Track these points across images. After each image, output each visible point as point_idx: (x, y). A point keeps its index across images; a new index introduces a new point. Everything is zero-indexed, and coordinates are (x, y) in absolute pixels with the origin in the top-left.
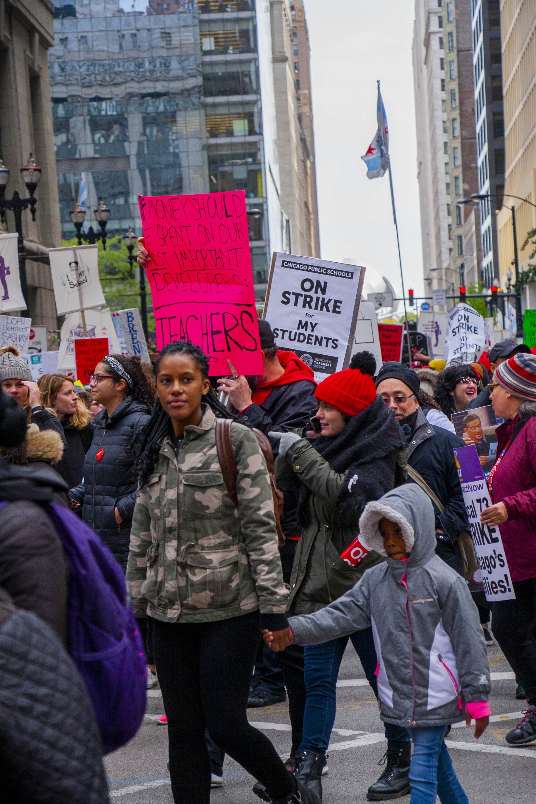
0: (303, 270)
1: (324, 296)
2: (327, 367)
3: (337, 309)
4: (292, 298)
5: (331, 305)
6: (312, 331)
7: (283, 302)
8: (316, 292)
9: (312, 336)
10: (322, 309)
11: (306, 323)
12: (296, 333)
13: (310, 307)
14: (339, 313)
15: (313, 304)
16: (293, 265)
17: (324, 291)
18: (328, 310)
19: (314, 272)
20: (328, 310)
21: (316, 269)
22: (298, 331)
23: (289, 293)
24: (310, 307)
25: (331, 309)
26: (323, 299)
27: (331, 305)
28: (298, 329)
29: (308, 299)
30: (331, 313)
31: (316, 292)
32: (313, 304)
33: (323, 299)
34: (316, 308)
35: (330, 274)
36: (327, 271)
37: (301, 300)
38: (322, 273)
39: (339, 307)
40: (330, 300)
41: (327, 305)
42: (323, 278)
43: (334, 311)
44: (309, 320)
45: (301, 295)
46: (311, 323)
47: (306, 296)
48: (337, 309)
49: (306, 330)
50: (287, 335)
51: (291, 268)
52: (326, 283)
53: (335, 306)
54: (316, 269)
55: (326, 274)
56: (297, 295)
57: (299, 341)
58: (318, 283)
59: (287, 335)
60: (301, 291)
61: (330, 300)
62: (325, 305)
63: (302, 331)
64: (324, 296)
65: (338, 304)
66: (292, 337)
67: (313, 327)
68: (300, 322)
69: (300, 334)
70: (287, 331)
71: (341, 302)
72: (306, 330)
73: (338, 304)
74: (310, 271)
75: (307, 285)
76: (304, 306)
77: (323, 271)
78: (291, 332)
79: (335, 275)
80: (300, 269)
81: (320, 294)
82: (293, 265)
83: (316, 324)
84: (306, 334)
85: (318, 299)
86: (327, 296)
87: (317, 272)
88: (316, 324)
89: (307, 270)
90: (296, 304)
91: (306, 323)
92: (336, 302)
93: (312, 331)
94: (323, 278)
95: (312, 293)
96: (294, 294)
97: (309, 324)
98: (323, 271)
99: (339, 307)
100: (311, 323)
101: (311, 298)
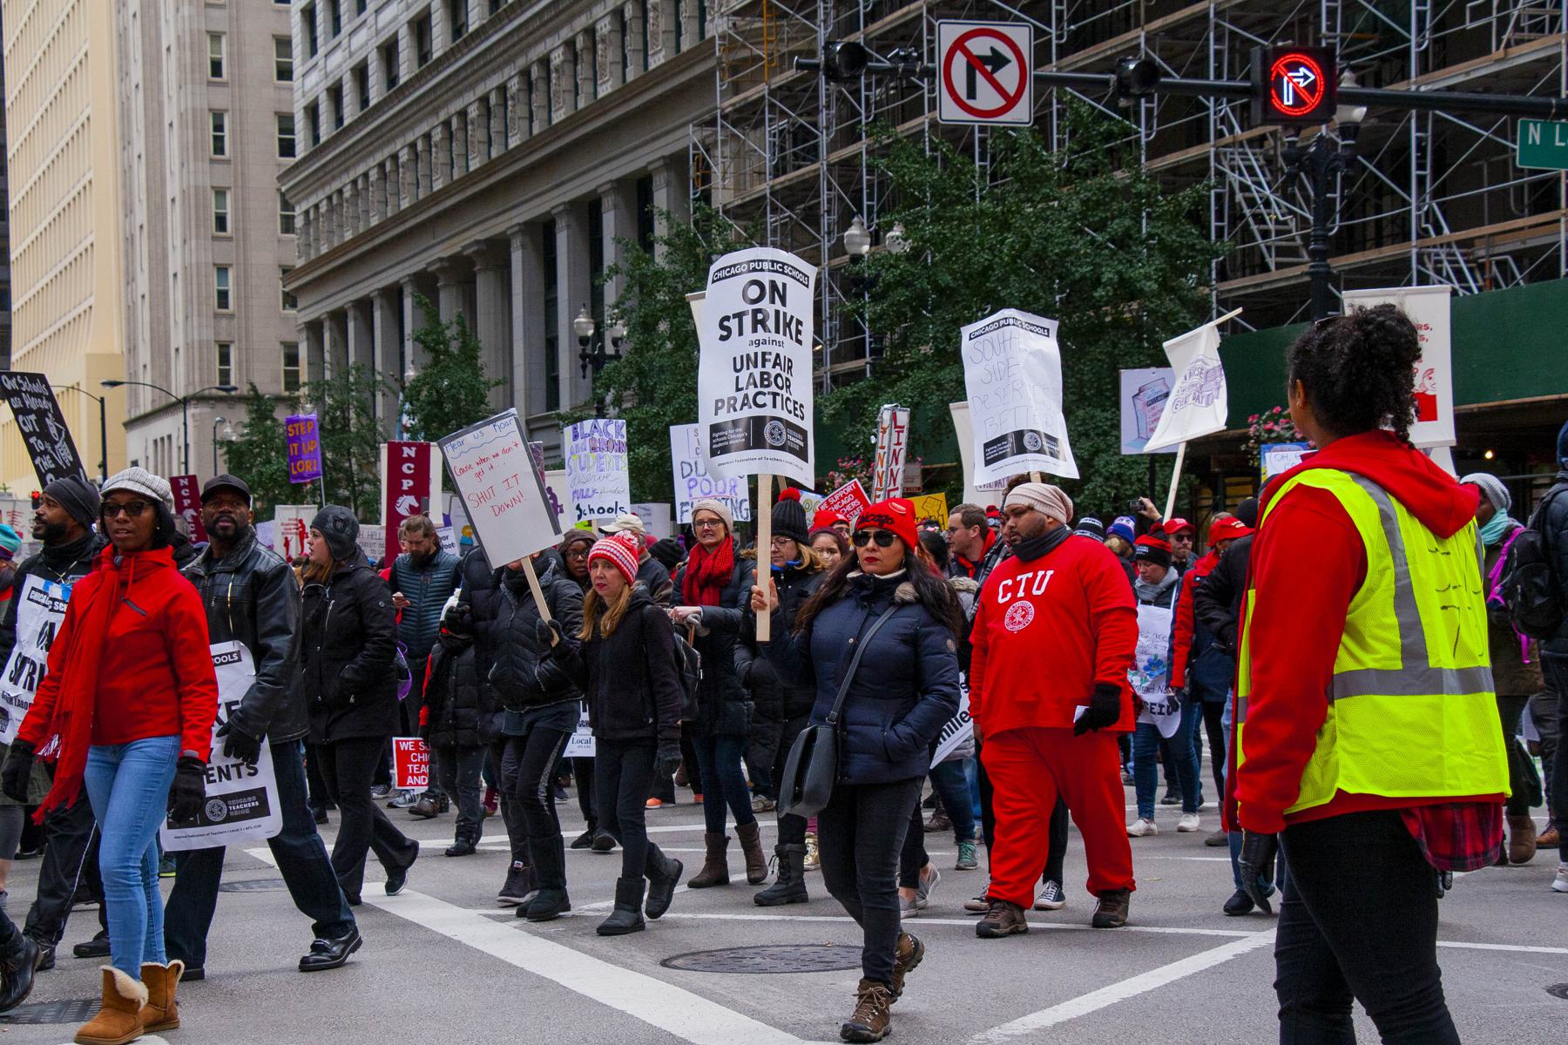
8: (773, 302)
13: (765, 329)
15: (771, 324)
26: (785, 314)
31: (773, 302)
32: (771, 324)
34: (777, 331)
37: (747, 320)
38: (777, 271)
52: (784, 285)
56: (739, 316)
76: (755, 330)
77: (777, 267)
85: (777, 312)
95: (765, 304)
96: (735, 316)
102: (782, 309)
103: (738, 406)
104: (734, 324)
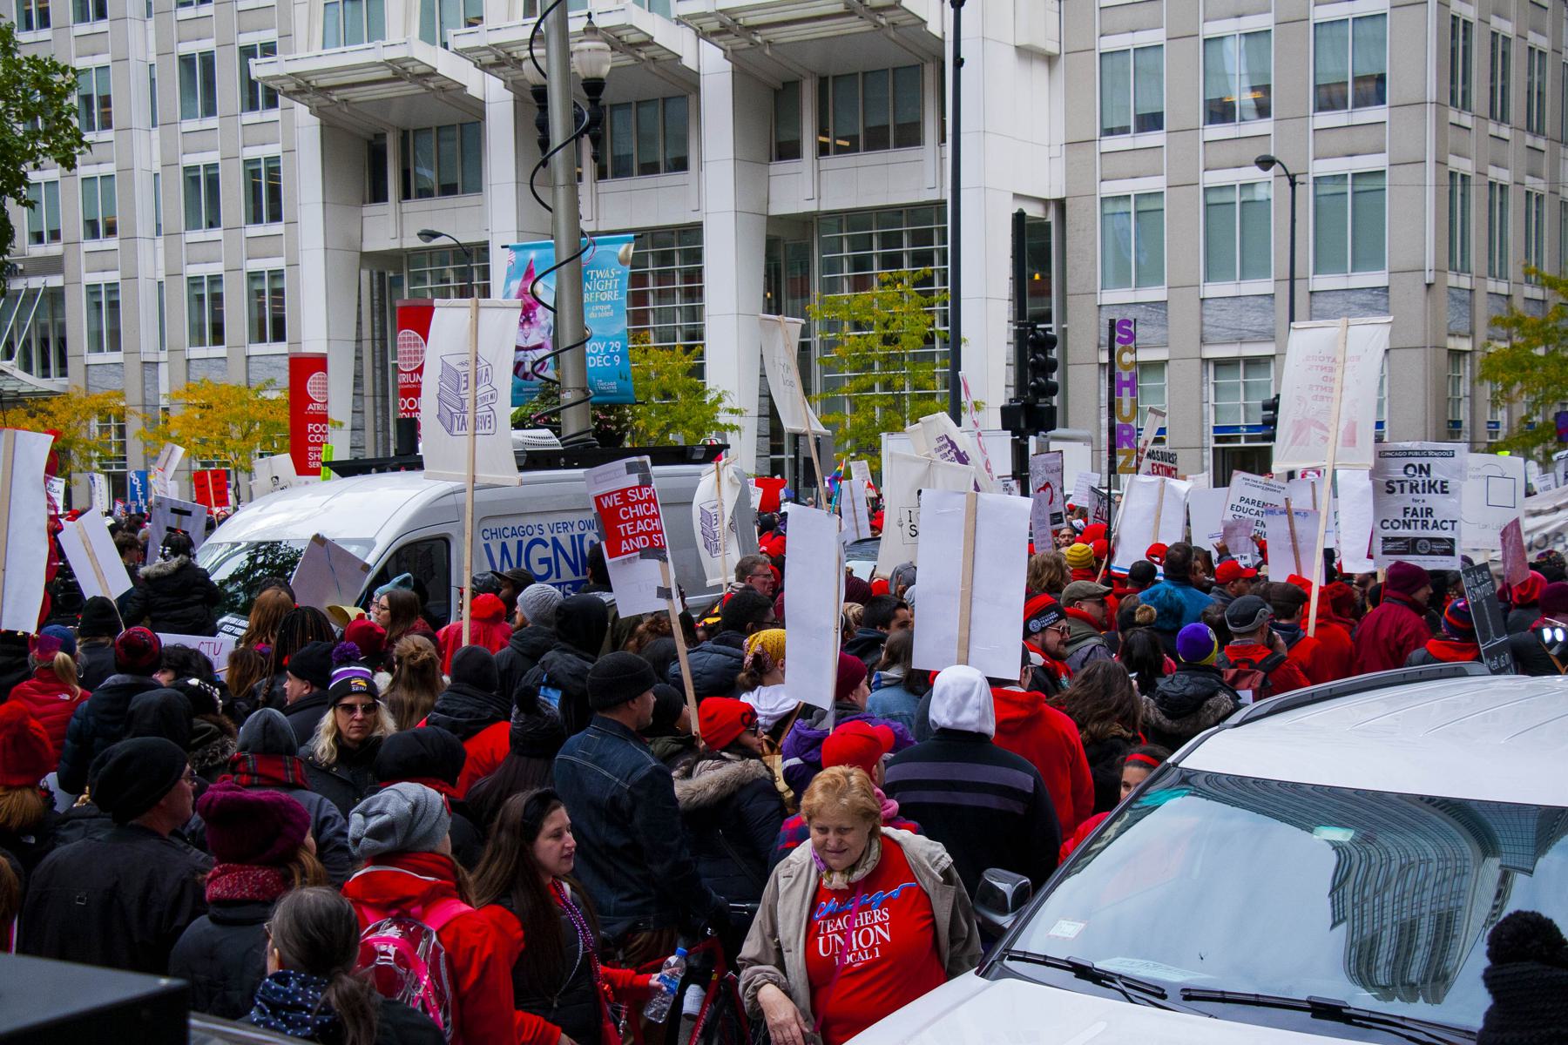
2: (1446, 550)
4: (1398, 486)
5: (1438, 486)
7: (1388, 492)
10: (1430, 492)
13: (1418, 492)
14: (1447, 492)
15: (1420, 488)
17: (1428, 473)
18: (1436, 492)
20: (1436, 492)
21: (1416, 454)
23: (1392, 482)
24: (1418, 492)
25: (1439, 490)
26: (1430, 482)
27: (1438, 486)
30: (1440, 495)
32: (1420, 488)
33: (1430, 482)
34: (1424, 492)
37: (1407, 486)
39: (1446, 487)
40: (1436, 482)
41: (1433, 486)
43: (1443, 492)
52: (1429, 465)
53: (1442, 486)
58: (1421, 466)
60: (1403, 476)
61: (1436, 482)
62: (1432, 486)
76: (1411, 492)
77: (1423, 453)
90: (1402, 492)
92: (1442, 482)
94: (1424, 461)
96: (1398, 481)
99: (1446, 487)
103: (1430, 525)
104: (1398, 486)
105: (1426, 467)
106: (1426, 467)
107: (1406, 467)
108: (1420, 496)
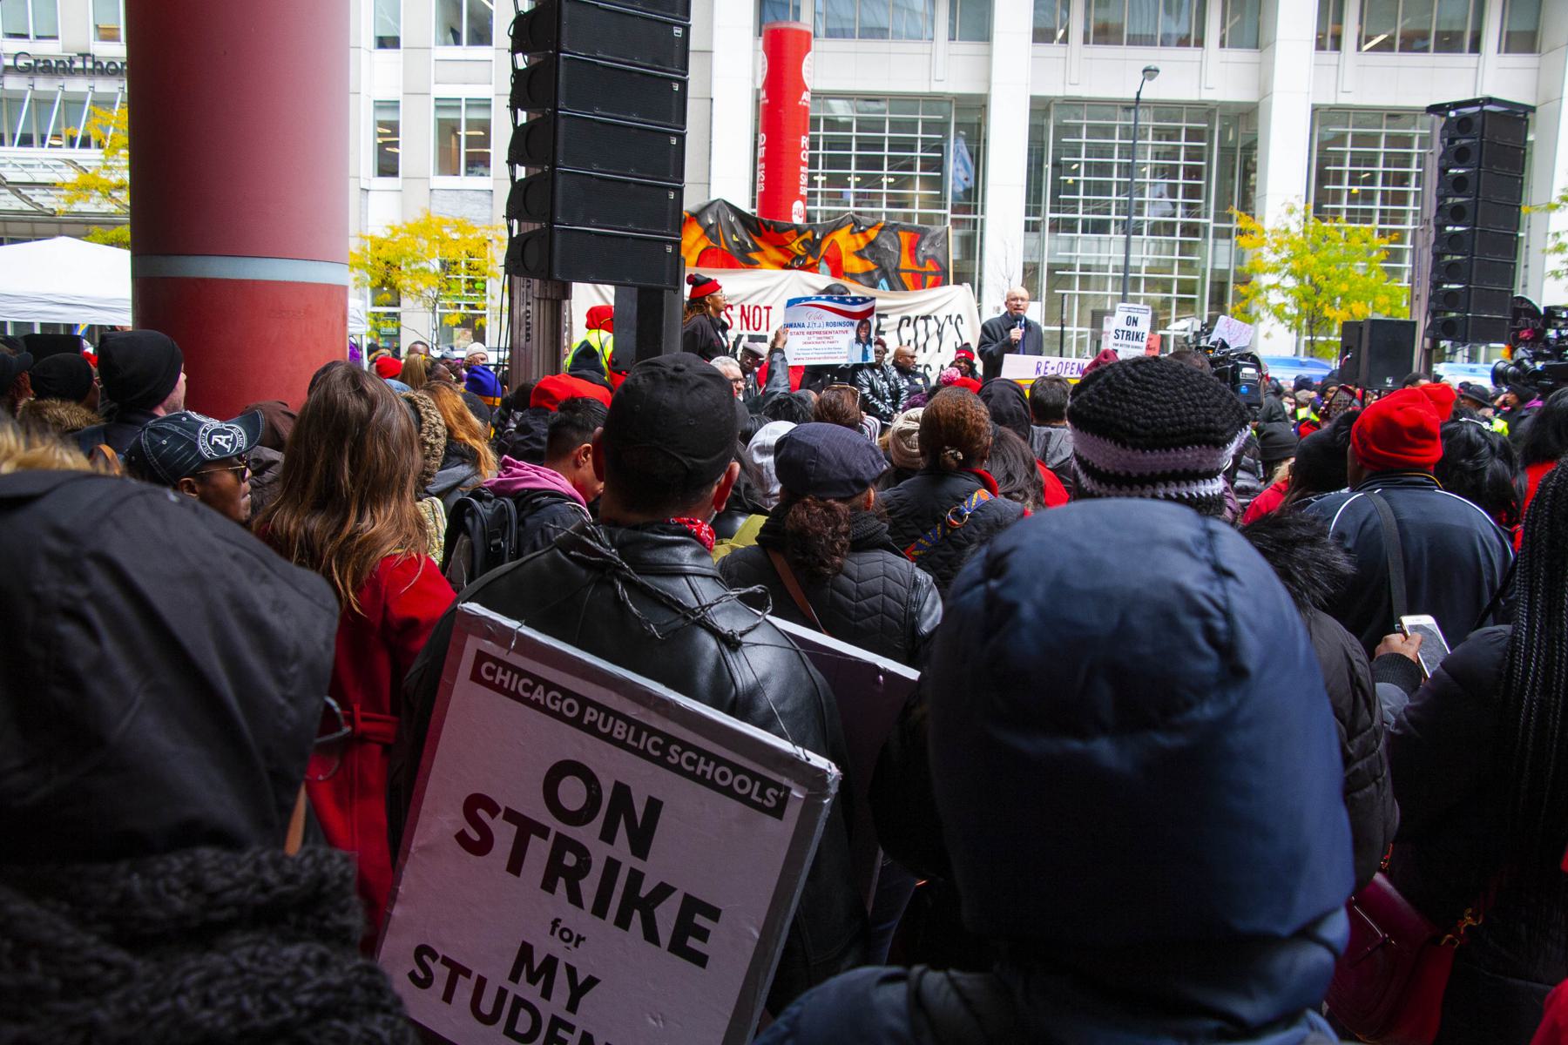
0: (559, 716)
1: (638, 864)
3: (693, 943)
4: (505, 836)
5: (667, 916)
6: (572, 1007)
7: (462, 838)
8: (608, 836)
9: (570, 1028)
10: (623, 922)
11: (550, 962)
12: (502, 993)
13: (575, 898)
14: (700, 960)
15: (589, 886)
16: (519, 685)
18: (651, 935)
19: (608, 738)
20: (651, 935)
22: (513, 990)
23: (493, 809)
25: (665, 932)
26: (636, 878)
27: (667, 916)
28: (514, 977)
29: (570, 860)
31: (608, 836)
32: (589, 886)
34: (600, 910)
35: (677, 769)
36: (664, 750)
37: (539, 851)
38: (644, 754)
39: (703, 935)
40: (663, 891)
41: (647, 908)
42: (645, 780)
44: (565, 955)
45: (543, 832)
46: (571, 971)
47: (562, 844)
48: (693, 943)
49: (546, 994)
50: (464, 989)
51: (506, 693)
52: (654, 806)
53: (685, 927)
54: (620, 730)
55: (662, 762)
56: (527, 828)
57: (510, 1031)
58: (621, 792)
59: (464, 989)
61: (663, 891)
63: (531, 993)
64: (638, 864)
65: (700, 920)
66: (487, 1006)
67: (579, 990)
68: (526, 951)
69: (519, 1003)
70: (468, 973)
71: (714, 913)
72: (546, 994)
73: (700, 920)
74: (591, 729)
75: (572, 793)
76: (548, 885)
77: (645, 742)
78: (481, 982)
79: (701, 779)
80: (544, 709)
81: (621, 848)
82: (519, 685)
83: (592, 982)
84: (547, 1009)
85: (612, 866)
86: (654, 872)
87: (622, 744)
88: (592, 982)
89: (577, 722)
90: (515, 866)
91: (550, 962)
92: (692, 905)
93: (572, 1007)
94: (645, 780)
97: (561, 975)
98: (645, 742)
99: (703, 935)
100: (571, 971)
101: (582, 852)
102: (628, 861)
105: (640, 809)
106: (640, 809)
107: (565, 768)
108: (579, 919)
